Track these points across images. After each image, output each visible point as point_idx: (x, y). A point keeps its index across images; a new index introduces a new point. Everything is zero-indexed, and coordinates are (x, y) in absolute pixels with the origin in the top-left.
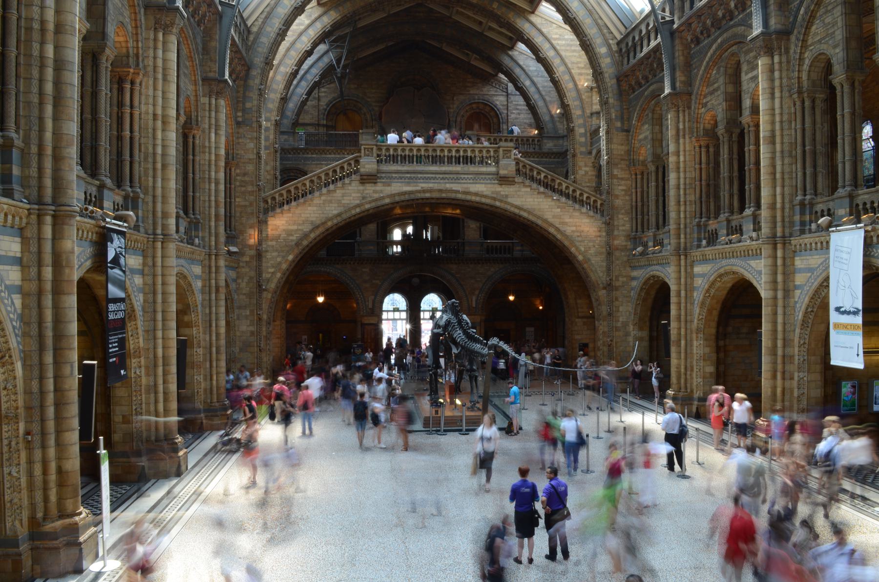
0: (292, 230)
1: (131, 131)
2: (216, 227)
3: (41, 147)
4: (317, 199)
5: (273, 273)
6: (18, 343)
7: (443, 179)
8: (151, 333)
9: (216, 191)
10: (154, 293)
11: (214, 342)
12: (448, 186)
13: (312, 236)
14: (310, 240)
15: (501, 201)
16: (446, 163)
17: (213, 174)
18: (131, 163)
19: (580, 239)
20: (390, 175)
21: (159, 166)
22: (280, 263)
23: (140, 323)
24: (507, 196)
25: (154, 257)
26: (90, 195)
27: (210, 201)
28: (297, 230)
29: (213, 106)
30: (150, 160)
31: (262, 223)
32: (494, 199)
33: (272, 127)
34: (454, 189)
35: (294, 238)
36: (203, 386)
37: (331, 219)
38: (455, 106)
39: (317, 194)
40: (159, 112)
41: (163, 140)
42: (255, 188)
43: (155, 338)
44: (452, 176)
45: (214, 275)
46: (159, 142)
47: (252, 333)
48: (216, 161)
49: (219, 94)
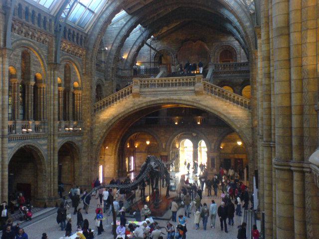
2: (54, 123)
5: (98, 137)
7: (169, 94)
9: (54, 109)
11: (52, 171)
12: (172, 97)
15: (196, 103)
17: (52, 102)
19: (237, 121)
22: (100, 133)
24: (199, 101)
27: (51, 113)
29: (52, 74)
32: (193, 102)
34: (174, 98)
36: (47, 188)
38: (214, 48)
44: (173, 92)
45: (52, 143)
48: (54, 96)
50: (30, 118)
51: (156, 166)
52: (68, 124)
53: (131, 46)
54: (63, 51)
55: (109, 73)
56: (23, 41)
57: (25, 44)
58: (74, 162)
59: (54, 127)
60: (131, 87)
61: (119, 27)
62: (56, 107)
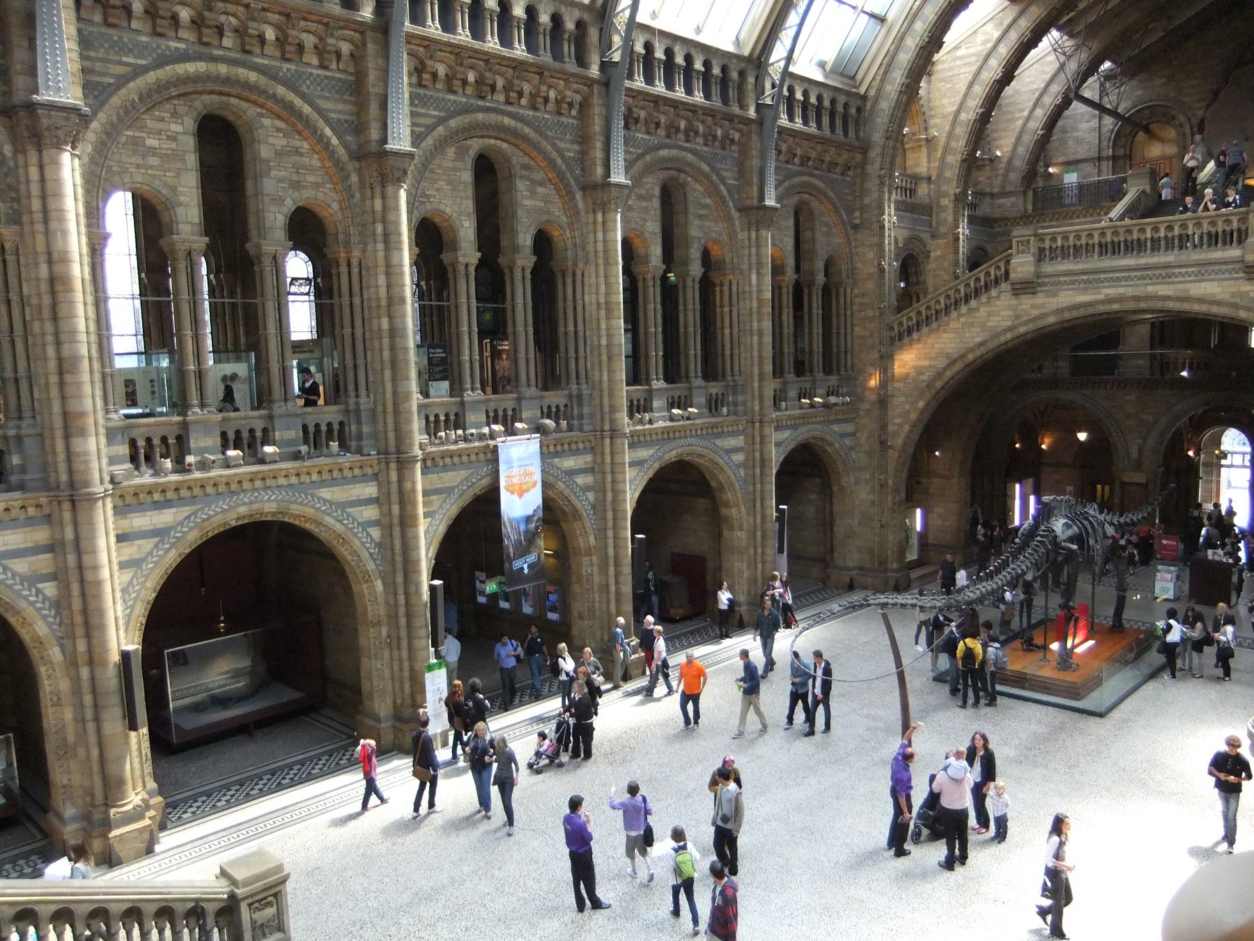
0: (923, 367)
1: (576, 325)
3: (384, 405)
4: (956, 321)
5: (900, 425)
6: (377, 566)
8: (601, 532)
9: (760, 344)
10: (604, 492)
11: (759, 526)
13: (949, 374)
14: (945, 380)
16: (1148, 251)
17: (755, 324)
18: (577, 359)
20: (1056, 279)
21: (604, 358)
23: (587, 523)
25: (603, 455)
26: (505, 410)
28: (930, 366)
30: (595, 352)
31: (885, 360)
33: (951, 205)
35: (925, 377)
36: (746, 575)
37: (971, 350)
39: (954, 314)
40: (602, 300)
41: (608, 329)
42: (877, 313)
43: (606, 537)
45: (758, 446)
46: (603, 332)
47: (873, 503)
48: (759, 307)
49: (759, 225)
50: (692, 374)
51: (1070, 533)
52: (808, 386)
53: (1026, 113)
54: (787, 162)
55: (943, 215)
56: (664, 153)
57: (671, 159)
58: (831, 497)
59: (761, 398)
60: (1008, 262)
61: (977, 55)
62: (768, 339)
